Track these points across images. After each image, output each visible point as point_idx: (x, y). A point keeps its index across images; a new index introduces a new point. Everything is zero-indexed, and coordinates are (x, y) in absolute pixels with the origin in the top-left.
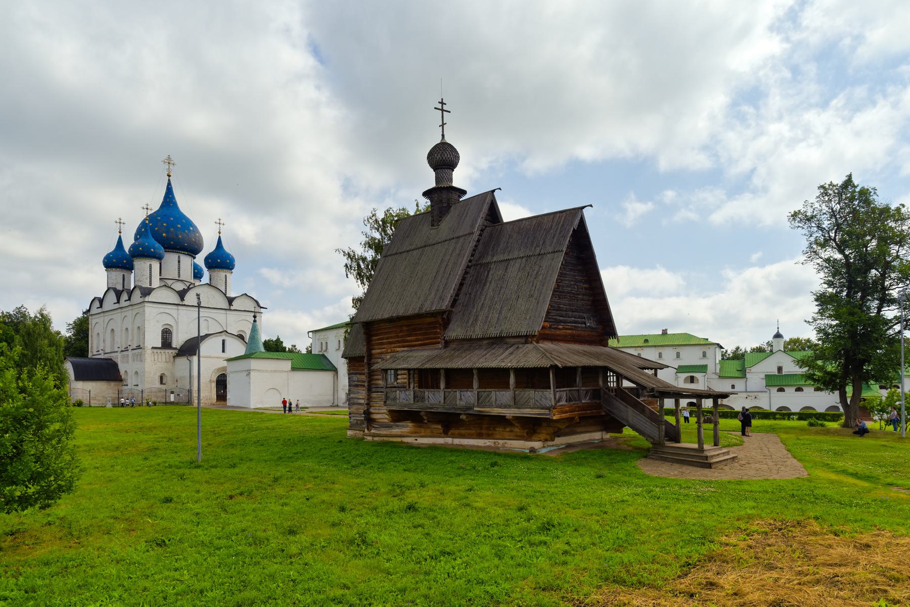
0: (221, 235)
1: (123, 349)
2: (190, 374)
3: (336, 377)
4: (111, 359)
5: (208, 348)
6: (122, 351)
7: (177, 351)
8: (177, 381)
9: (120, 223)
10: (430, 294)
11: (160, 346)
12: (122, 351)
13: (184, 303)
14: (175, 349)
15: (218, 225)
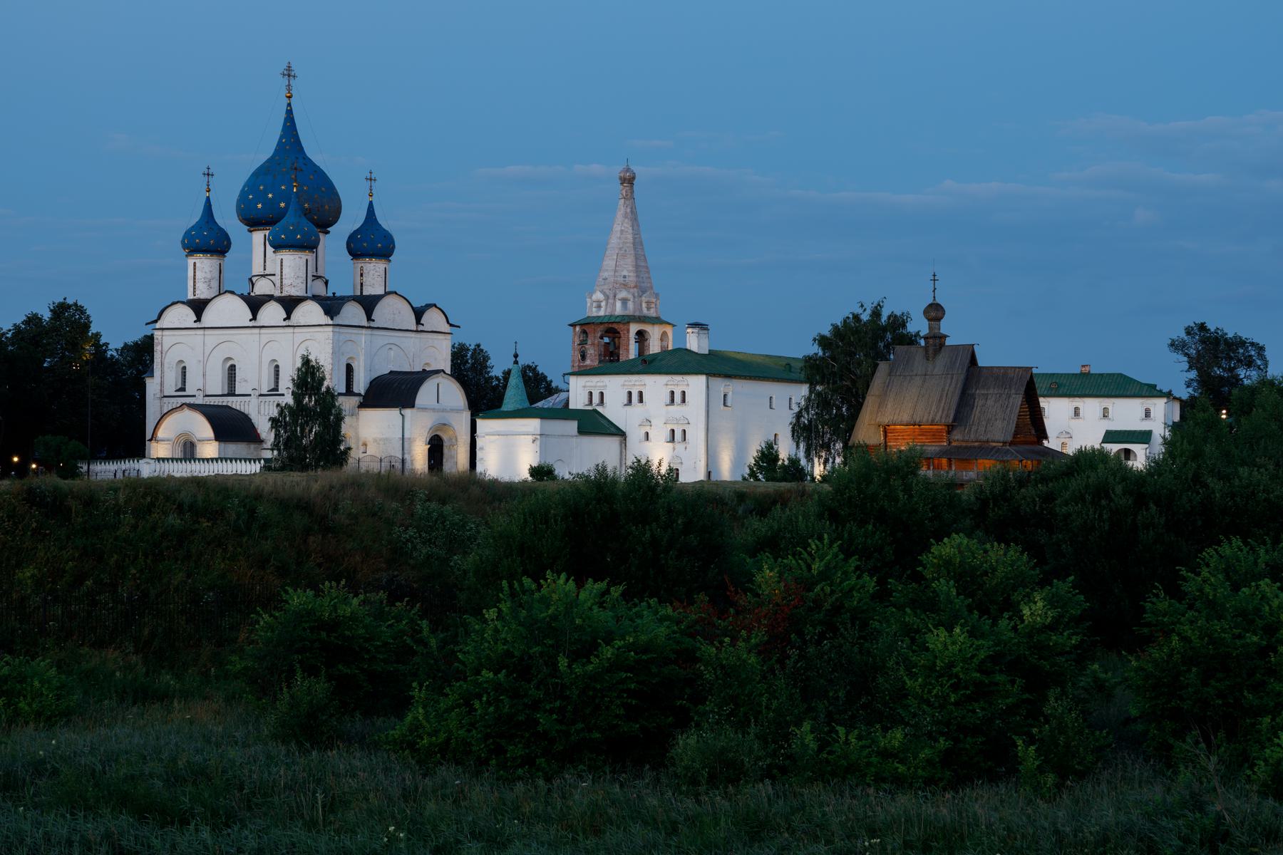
0: (374, 199)
1: (265, 392)
2: (403, 436)
3: (623, 445)
4: (227, 407)
5: (425, 394)
6: (261, 395)
7: (361, 399)
8: (365, 445)
9: (208, 175)
10: (938, 411)
11: (345, 392)
12: (261, 395)
13: (372, 324)
14: (359, 395)
15: (369, 181)
